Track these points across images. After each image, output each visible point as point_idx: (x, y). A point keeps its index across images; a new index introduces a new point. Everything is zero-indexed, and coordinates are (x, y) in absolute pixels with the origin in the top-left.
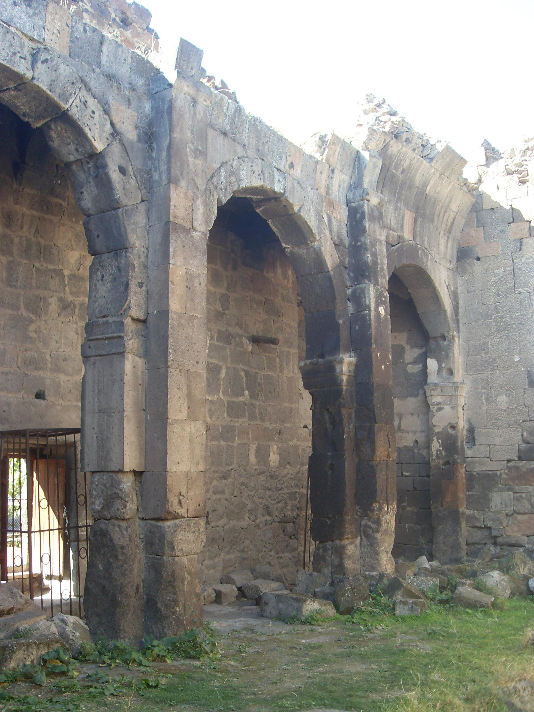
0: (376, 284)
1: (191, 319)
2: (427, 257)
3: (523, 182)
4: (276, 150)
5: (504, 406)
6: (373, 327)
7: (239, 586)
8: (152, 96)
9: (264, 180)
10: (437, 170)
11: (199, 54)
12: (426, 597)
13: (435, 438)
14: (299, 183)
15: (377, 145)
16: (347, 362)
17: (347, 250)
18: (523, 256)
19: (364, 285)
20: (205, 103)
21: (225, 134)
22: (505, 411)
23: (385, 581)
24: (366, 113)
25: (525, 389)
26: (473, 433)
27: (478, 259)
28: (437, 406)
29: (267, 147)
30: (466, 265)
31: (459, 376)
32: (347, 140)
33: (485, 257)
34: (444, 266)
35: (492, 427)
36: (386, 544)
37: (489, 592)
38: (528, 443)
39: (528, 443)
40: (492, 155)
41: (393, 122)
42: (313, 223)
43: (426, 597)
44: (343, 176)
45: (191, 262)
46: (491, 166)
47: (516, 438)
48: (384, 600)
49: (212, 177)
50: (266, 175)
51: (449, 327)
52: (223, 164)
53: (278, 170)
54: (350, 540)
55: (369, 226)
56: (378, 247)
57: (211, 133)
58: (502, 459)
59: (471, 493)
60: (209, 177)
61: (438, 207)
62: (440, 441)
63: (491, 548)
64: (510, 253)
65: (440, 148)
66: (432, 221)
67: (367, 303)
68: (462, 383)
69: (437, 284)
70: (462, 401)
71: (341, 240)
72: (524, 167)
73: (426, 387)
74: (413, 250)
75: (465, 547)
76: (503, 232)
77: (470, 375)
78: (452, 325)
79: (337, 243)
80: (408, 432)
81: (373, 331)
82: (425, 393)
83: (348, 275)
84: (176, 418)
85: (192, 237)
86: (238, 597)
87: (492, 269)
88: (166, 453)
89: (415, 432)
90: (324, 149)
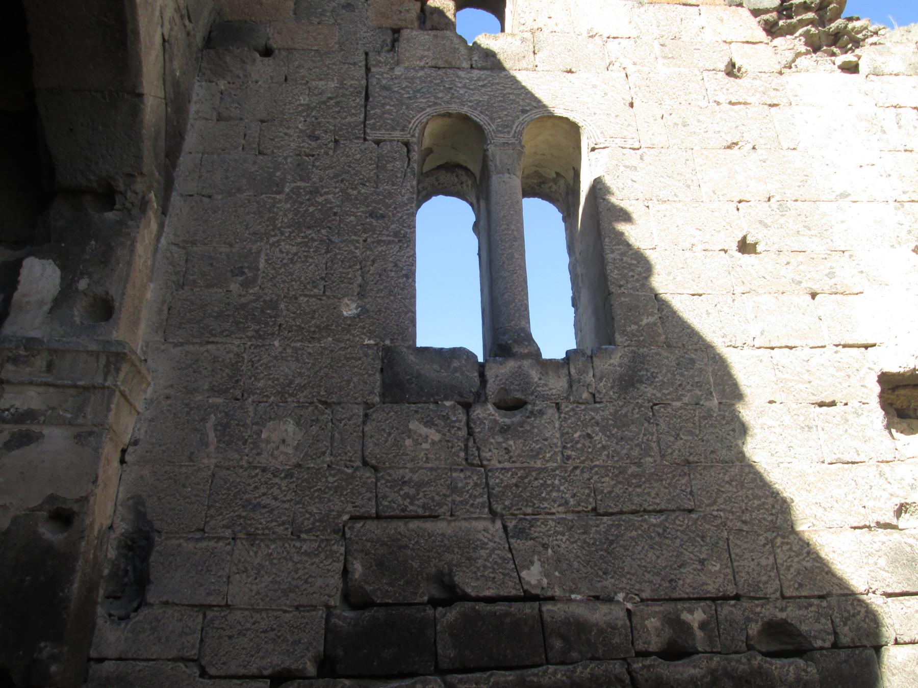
18: (398, 63)
22: (289, 475)
25: (368, 405)
26: (145, 559)
27: (267, 52)
28: (16, 428)
30: (228, 58)
33: (289, 50)
35: (228, 533)
47: (319, 582)
51: (139, 157)
58: (254, 670)
64: (362, 51)
70: (126, 424)
77: (175, 345)
87: (303, 78)
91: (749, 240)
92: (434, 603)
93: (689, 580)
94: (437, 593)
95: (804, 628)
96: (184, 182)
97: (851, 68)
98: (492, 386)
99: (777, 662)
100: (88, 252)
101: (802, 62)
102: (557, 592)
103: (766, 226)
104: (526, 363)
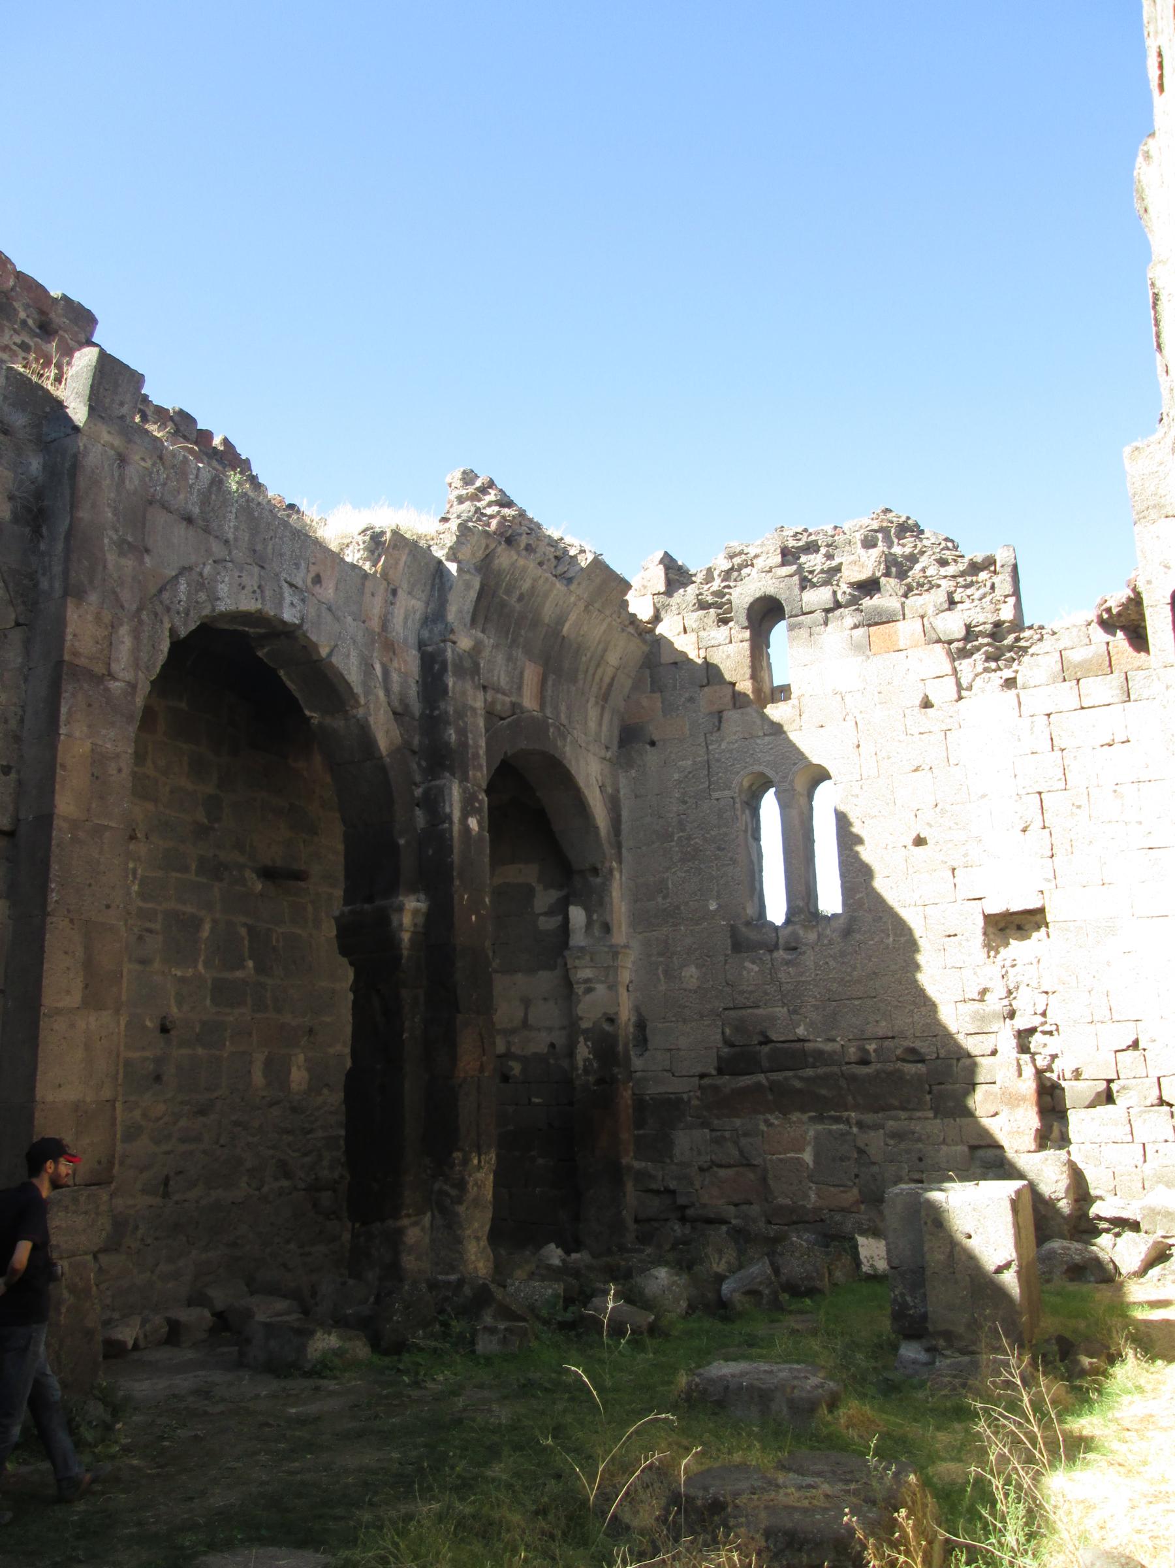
0: (464, 778)
1: (99, 831)
2: (565, 739)
3: (724, 621)
4: (288, 553)
5: (693, 983)
6: (456, 851)
7: (219, 1305)
8: (44, 445)
9: (263, 598)
10: (579, 598)
11: (138, 379)
12: (538, 1318)
13: (581, 1039)
14: (329, 609)
15: (473, 554)
16: (411, 910)
17: (416, 723)
19: (444, 781)
20: (143, 464)
21: (189, 520)
22: (695, 992)
23: (467, 1291)
24: (461, 500)
25: (726, 955)
27: (653, 744)
29: (270, 547)
31: (622, 933)
32: (422, 543)
34: (594, 754)
36: (476, 1225)
37: (647, 1304)
38: (732, 1045)
39: (732, 1045)
40: (676, 576)
41: (504, 517)
42: (353, 675)
43: (538, 1318)
44: (413, 602)
45: (104, 732)
46: (675, 595)
48: (457, 1326)
49: (160, 591)
50: (268, 593)
52: (184, 570)
53: (291, 585)
54: (413, 1219)
55: (454, 683)
56: (469, 720)
57: (159, 518)
59: (641, 1132)
60: (153, 591)
61: (584, 659)
62: (589, 1043)
63: (676, 1227)
65: (584, 561)
66: (574, 681)
67: (448, 810)
68: (626, 947)
69: (582, 783)
70: (625, 976)
71: (407, 707)
72: (727, 597)
73: (567, 953)
74: (540, 727)
75: (632, 1226)
76: (691, 700)
78: (609, 851)
79: (399, 710)
80: (539, 1030)
81: (456, 857)
82: (566, 964)
83: (419, 765)
84: (60, 1005)
85: (107, 690)
86: (212, 1331)
88: (35, 1069)
89: (550, 1029)
90: (380, 556)
91: (922, 836)
92: (761, 1043)
93: (870, 1030)
94: (762, 1039)
95: (923, 1050)
96: (627, 842)
97: (1010, 683)
98: (781, 941)
99: (910, 1065)
100: (595, 901)
101: (978, 683)
102: (811, 1037)
103: (931, 826)
104: (797, 927)
